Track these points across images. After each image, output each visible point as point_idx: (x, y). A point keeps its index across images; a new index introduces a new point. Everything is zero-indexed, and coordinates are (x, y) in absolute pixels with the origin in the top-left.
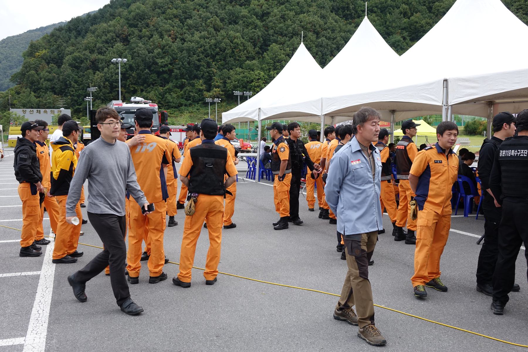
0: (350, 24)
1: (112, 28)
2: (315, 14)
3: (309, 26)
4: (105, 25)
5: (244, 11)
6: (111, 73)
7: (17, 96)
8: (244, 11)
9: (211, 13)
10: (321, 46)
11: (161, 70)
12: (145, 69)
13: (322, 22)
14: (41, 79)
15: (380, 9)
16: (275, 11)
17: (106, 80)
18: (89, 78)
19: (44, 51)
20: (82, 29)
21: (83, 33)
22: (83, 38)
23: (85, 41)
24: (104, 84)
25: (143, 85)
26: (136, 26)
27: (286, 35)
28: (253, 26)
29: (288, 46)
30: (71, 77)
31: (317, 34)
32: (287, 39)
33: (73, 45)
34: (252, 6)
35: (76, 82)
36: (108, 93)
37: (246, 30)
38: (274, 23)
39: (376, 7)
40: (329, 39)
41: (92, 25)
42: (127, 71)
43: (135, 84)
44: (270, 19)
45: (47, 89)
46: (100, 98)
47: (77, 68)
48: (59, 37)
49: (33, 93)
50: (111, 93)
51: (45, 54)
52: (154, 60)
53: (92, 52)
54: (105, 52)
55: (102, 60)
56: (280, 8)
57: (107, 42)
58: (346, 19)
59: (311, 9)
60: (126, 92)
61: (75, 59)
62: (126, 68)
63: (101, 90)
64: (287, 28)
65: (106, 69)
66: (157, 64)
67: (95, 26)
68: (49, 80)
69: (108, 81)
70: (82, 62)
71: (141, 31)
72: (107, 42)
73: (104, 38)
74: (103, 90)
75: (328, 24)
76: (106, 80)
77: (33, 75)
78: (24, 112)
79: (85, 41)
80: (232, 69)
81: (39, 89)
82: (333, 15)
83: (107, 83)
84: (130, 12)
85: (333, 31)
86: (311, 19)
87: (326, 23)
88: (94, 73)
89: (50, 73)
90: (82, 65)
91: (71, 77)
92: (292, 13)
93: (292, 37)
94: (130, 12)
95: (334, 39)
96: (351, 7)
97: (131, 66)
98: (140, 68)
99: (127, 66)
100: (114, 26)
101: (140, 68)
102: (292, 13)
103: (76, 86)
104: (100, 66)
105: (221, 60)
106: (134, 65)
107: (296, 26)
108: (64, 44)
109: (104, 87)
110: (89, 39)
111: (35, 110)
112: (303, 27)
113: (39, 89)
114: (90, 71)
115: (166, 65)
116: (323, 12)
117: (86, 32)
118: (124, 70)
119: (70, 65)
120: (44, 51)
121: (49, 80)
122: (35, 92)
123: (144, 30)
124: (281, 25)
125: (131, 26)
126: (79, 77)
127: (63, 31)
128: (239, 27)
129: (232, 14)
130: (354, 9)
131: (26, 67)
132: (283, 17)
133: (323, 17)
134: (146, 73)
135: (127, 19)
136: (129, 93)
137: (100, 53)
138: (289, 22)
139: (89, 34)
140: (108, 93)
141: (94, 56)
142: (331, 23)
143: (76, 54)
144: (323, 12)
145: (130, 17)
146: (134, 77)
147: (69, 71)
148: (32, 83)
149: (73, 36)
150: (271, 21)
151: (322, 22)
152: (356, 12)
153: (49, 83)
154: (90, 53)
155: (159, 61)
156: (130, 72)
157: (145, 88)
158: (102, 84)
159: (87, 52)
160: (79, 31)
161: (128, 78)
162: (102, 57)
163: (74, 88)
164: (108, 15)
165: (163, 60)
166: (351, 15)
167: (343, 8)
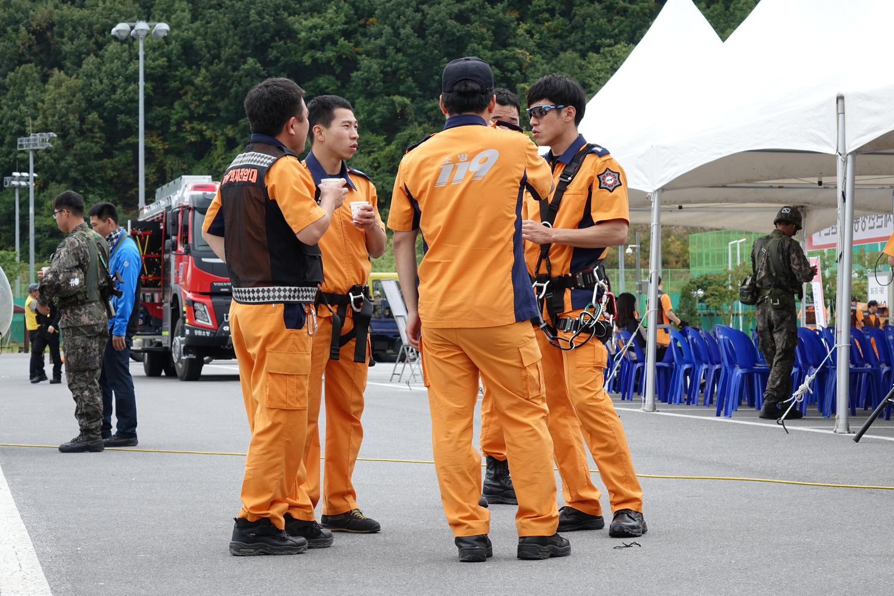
6: (111, 75)
11: (307, 59)
12: (243, 57)
17: (92, 105)
18: (22, 97)
24: (82, 120)
25: (234, 122)
36: (98, 157)
42: (171, 66)
43: (202, 118)
50: (107, 153)
52: (279, 20)
55: (76, 24)
60: (167, 152)
63: (68, 146)
65: (90, 62)
66: (291, 34)
74: (80, 145)
76: (92, 105)
80: (596, 49)
83: (94, 116)
88: (45, 79)
97: (187, 48)
98: (226, 53)
99: (175, 46)
101: (226, 53)
104: (67, 48)
105: (552, 12)
106: (199, 42)
109: (81, 133)
114: (29, 68)
115: (330, 39)
118: (162, 61)
134: (248, 74)
136: (179, 154)
140: (98, 157)
146: (200, 92)
155: (302, 24)
156: (184, 71)
158: (73, 119)
161: (177, 95)
165: (316, 20)
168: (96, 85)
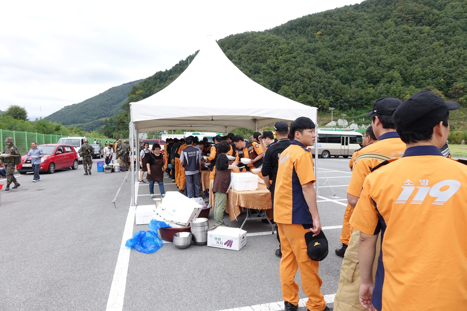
0: (329, 73)
2: (307, 67)
3: (305, 75)
5: (264, 66)
8: (264, 66)
9: (244, 67)
10: (313, 87)
13: (312, 72)
15: (346, 64)
16: (283, 65)
19: (141, 91)
20: (163, 78)
21: (164, 80)
27: (290, 80)
28: (270, 75)
29: (293, 87)
31: (310, 79)
32: (292, 82)
34: (268, 63)
37: (266, 77)
38: (283, 73)
39: (344, 63)
40: (318, 82)
41: (169, 75)
44: (280, 70)
51: (142, 93)
56: (286, 64)
58: (326, 71)
59: (304, 65)
64: (291, 76)
75: (316, 73)
82: (318, 68)
85: (320, 77)
86: (306, 71)
87: (315, 73)
92: (293, 67)
93: (295, 82)
95: (321, 82)
96: (328, 63)
102: (293, 67)
107: (297, 75)
112: (301, 75)
116: (312, 66)
117: (166, 80)
120: (141, 91)
124: (288, 74)
127: (152, 79)
128: (261, 75)
129: (256, 67)
130: (330, 64)
132: (288, 70)
133: (312, 69)
138: (292, 72)
142: (319, 73)
144: (312, 66)
150: (280, 72)
151: (312, 72)
152: (332, 66)
164: (179, 69)
166: (328, 68)
167: (323, 64)
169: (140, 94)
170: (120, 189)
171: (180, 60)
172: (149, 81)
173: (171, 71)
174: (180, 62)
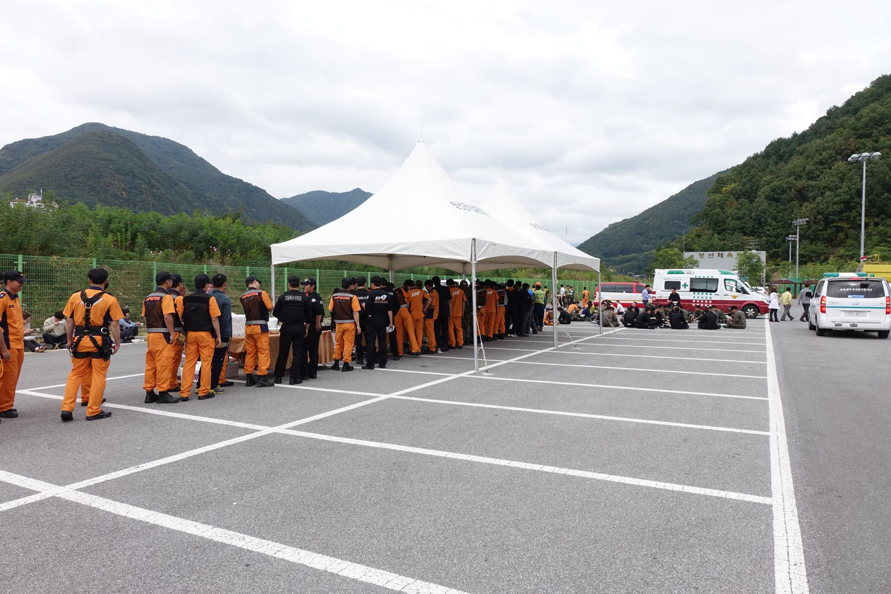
1: (830, 144)
4: (819, 141)
7: (696, 240)
12: (883, 194)
14: (727, 218)
17: (819, 213)
18: (793, 212)
19: (733, 185)
20: (785, 152)
22: (786, 162)
23: (790, 165)
24: (815, 218)
25: (878, 216)
26: (869, 136)
30: (768, 213)
33: (772, 172)
35: (774, 218)
36: (821, 230)
42: (852, 198)
45: (735, 229)
46: (808, 238)
47: (776, 200)
48: (753, 166)
49: (716, 235)
50: (825, 229)
51: (734, 188)
53: (798, 177)
54: (818, 176)
55: (813, 187)
57: (821, 163)
60: (849, 228)
61: (773, 190)
62: (851, 194)
65: (819, 199)
67: (803, 146)
68: (739, 219)
69: (819, 213)
70: (784, 192)
71: (877, 142)
72: (821, 163)
73: (817, 158)
74: (814, 227)
77: (718, 215)
78: (702, 256)
79: (790, 165)
81: (724, 230)
83: (820, 217)
84: (858, 119)
88: (801, 206)
89: (739, 209)
90: (784, 197)
91: (768, 213)
94: (858, 119)
98: (875, 192)
100: (833, 140)
101: (875, 192)
103: (774, 223)
108: (760, 174)
109: (815, 223)
110: (796, 161)
111: (716, 253)
113: (724, 230)
117: (791, 155)
118: (848, 196)
119: (767, 198)
121: (739, 219)
122: (719, 234)
123: (882, 139)
125: (860, 137)
126: (778, 212)
131: (710, 206)
134: (884, 199)
135: (854, 129)
137: (811, 178)
139: (795, 157)
140: (821, 230)
141: (800, 183)
143: (776, 183)
145: (859, 125)
147: (765, 204)
148: (716, 223)
149: (771, 161)
153: (738, 222)
154: (796, 179)
157: (882, 220)
159: (791, 179)
160: (780, 156)
162: (813, 183)
163: (770, 226)
164: (824, 128)
168: (821, 206)
169: (731, 192)
170: (291, 351)
171: (829, 106)
172: (752, 162)
173: (804, 134)
174: (829, 112)
